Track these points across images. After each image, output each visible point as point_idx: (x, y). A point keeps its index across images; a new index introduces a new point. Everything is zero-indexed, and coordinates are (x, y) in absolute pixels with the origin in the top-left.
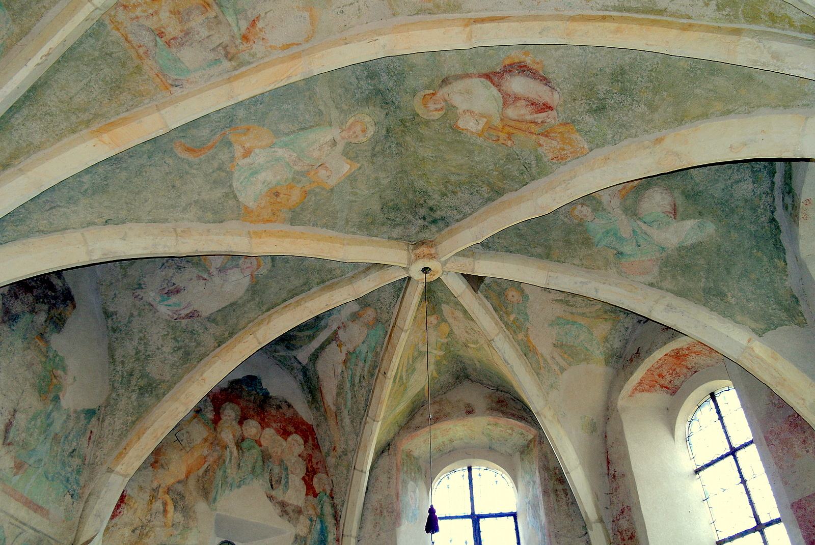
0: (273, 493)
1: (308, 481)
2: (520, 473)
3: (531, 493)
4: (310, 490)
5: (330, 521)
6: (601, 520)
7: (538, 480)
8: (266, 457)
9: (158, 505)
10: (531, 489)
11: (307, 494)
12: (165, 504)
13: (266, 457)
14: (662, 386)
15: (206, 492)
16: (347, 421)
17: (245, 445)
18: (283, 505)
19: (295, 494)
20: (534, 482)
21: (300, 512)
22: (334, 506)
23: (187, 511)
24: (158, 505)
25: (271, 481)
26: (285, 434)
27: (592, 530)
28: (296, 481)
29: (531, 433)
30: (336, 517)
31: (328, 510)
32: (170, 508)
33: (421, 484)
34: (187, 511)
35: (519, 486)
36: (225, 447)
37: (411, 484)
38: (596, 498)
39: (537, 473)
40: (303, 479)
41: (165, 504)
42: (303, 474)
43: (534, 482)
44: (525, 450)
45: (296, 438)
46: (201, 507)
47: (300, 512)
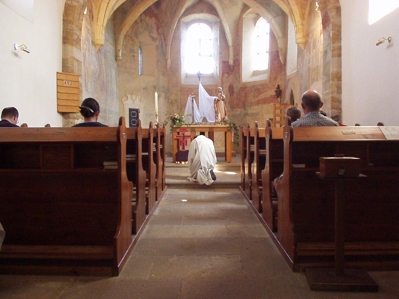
0: (151, 35)
1: (157, 30)
2: (213, 29)
3: (216, 36)
4: (158, 33)
5: (163, 40)
6: (233, 46)
7: (219, 33)
8: (147, 25)
9: (127, 40)
10: (216, 34)
11: (158, 34)
12: (129, 40)
13: (147, 25)
14: (255, 13)
15: (136, 35)
16: (168, 14)
17: (142, 22)
18: (153, 38)
19: (155, 35)
20: (217, 34)
21: (156, 39)
22: (164, 37)
23: (133, 41)
24: (127, 40)
25: (149, 31)
26: (151, 17)
27: (230, 48)
28: (155, 31)
29: (218, 20)
30: (165, 40)
31: (163, 38)
32: (130, 41)
33: (185, 29)
34: (133, 41)
35: (213, 32)
36: (138, 23)
37: (183, 30)
38: (232, 43)
39: (219, 31)
40: (157, 30)
41: (129, 40)
42: (156, 29)
43: (217, 34)
44: (215, 23)
45: (154, 18)
46: (136, 39)
47: (156, 39)
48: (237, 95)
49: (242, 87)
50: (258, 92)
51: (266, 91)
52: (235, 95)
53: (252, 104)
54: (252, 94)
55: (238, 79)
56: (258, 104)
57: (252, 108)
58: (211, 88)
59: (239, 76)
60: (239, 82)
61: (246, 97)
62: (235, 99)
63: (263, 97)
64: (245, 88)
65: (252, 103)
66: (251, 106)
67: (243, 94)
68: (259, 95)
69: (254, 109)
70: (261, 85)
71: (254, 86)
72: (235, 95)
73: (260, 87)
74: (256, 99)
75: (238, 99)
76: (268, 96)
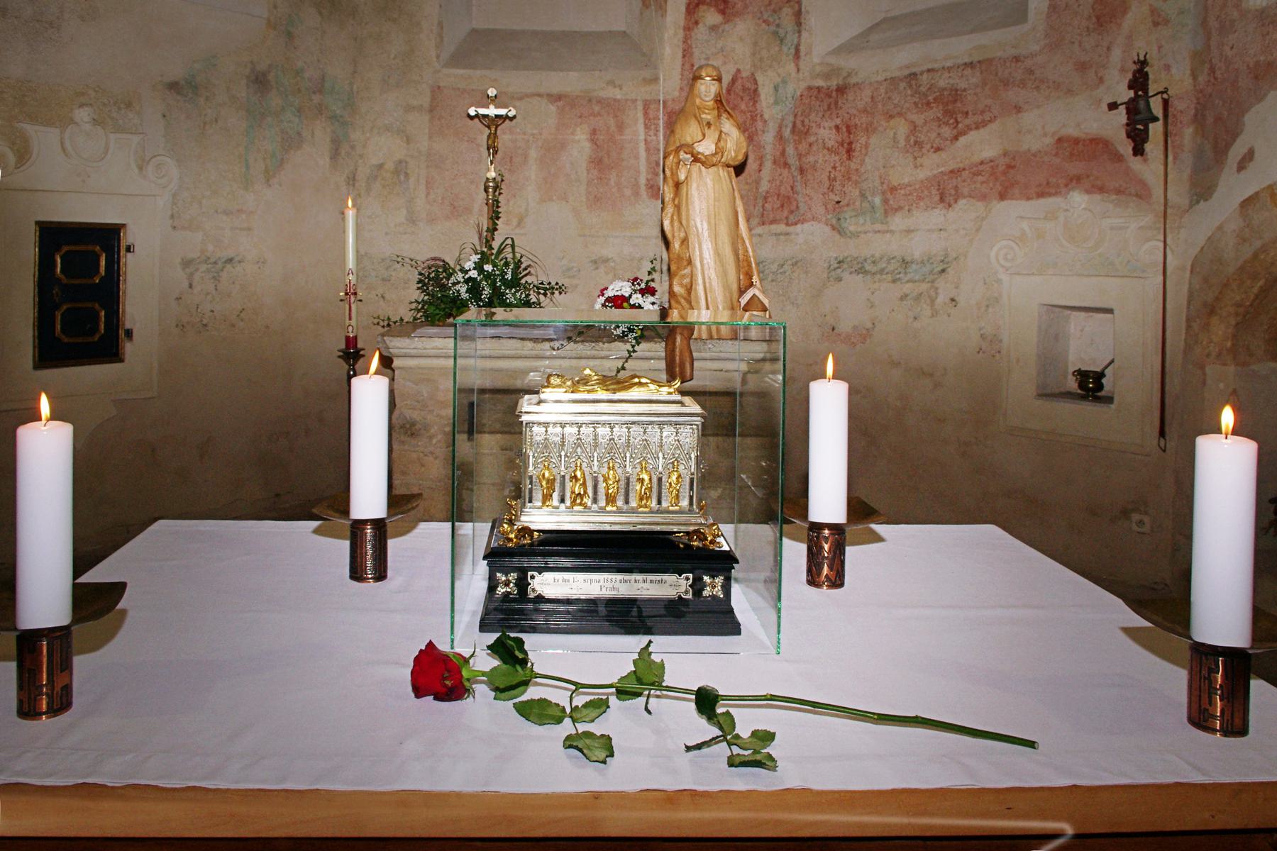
48: (780, 137)
49: (820, 83)
50: (946, 112)
51: (1018, 109)
52: (768, 138)
53: (894, 199)
54: (902, 128)
55: (792, 38)
56: (942, 200)
57: (898, 222)
58: (617, 94)
59: (798, 14)
60: (797, 55)
61: (849, 151)
62: (768, 165)
63: (988, 153)
64: (841, 90)
65: (893, 189)
66: (889, 210)
67: (826, 133)
68: (956, 138)
69: (909, 231)
70: (970, 65)
71: (914, 75)
72: (768, 138)
73: (962, 84)
74: (932, 165)
75: (786, 165)
76: (1035, 142)
